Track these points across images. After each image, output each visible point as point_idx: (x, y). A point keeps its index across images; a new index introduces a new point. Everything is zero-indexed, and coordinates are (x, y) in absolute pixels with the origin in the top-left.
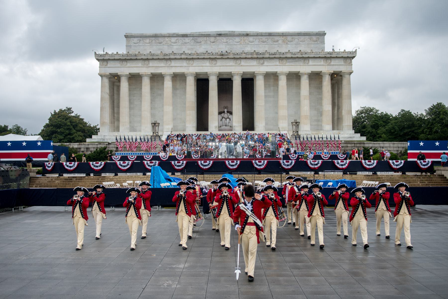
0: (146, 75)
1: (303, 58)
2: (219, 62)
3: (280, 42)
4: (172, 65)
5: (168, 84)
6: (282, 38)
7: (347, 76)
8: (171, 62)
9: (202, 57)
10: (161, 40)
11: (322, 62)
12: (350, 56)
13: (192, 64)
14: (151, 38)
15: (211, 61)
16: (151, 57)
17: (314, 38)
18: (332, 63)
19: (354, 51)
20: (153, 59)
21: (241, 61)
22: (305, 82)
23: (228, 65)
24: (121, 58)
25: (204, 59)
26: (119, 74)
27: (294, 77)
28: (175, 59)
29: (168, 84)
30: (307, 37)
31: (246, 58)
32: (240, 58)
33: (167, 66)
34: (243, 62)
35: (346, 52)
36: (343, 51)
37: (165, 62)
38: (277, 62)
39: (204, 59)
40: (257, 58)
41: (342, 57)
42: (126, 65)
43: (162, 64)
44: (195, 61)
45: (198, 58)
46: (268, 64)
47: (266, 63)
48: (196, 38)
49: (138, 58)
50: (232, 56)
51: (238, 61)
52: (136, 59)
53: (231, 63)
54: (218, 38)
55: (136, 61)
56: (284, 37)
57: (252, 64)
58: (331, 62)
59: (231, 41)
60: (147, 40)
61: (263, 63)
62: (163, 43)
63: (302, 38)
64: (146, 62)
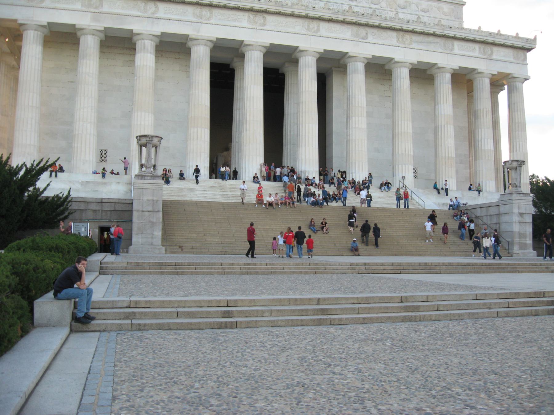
1: (444, 36)
4: (158, 15)
8: (157, 7)
11: (476, 49)
12: (526, 46)
13: (209, 19)
15: (252, 17)
18: (494, 57)
19: (532, 38)
21: (318, 26)
23: (290, 30)
31: (331, 21)
32: (320, 19)
33: (146, 15)
35: (519, 38)
36: (514, 35)
40: (356, 24)
44: (216, 11)
46: (375, 41)
47: (370, 39)
50: (303, 12)
51: (314, 25)
57: (342, 36)
58: (492, 53)
61: (366, 37)
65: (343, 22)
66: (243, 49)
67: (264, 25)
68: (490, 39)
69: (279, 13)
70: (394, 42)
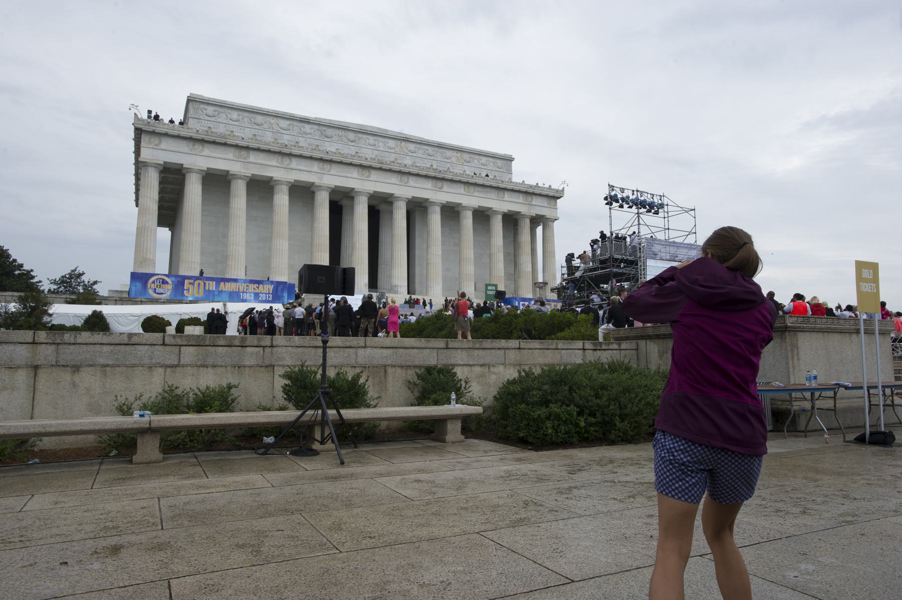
0: (240, 177)
1: (498, 188)
2: (374, 175)
3: (454, 159)
5: (282, 199)
6: (455, 153)
7: (550, 223)
9: (348, 160)
10: (259, 119)
11: (521, 198)
12: (557, 195)
14: (241, 113)
15: (360, 170)
16: (255, 145)
17: (500, 163)
19: (561, 188)
20: (258, 150)
22: (497, 225)
23: (388, 181)
24: (194, 135)
25: (351, 164)
26: (185, 166)
27: (482, 216)
28: (301, 156)
29: (282, 199)
30: (491, 159)
31: (417, 175)
32: (409, 174)
34: (412, 181)
37: (280, 158)
38: (461, 189)
39: (351, 164)
41: (547, 196)
42: (202, 151)
43: (274, 161)
44: (334, 166)
45: (341, 163)
46: (448, 190)
48: (323, 128)
49: (229, 142)
51: (405, 178)
52: (225, 144)
53: (394, 179)
54: (360, 135)
55: (223, 148)
56: (459, 154)
57: (425, 186)
59: (381, 144)
60: (235, 115)
61: (442, 188)
62: (264, 126)
63: (484, 160)
64: (244, 153)
65: (426, 177)
66: (353, 194)
67: (369, 176)
68: (531, 190)
69: (380, 169)
70: (462, 191)
